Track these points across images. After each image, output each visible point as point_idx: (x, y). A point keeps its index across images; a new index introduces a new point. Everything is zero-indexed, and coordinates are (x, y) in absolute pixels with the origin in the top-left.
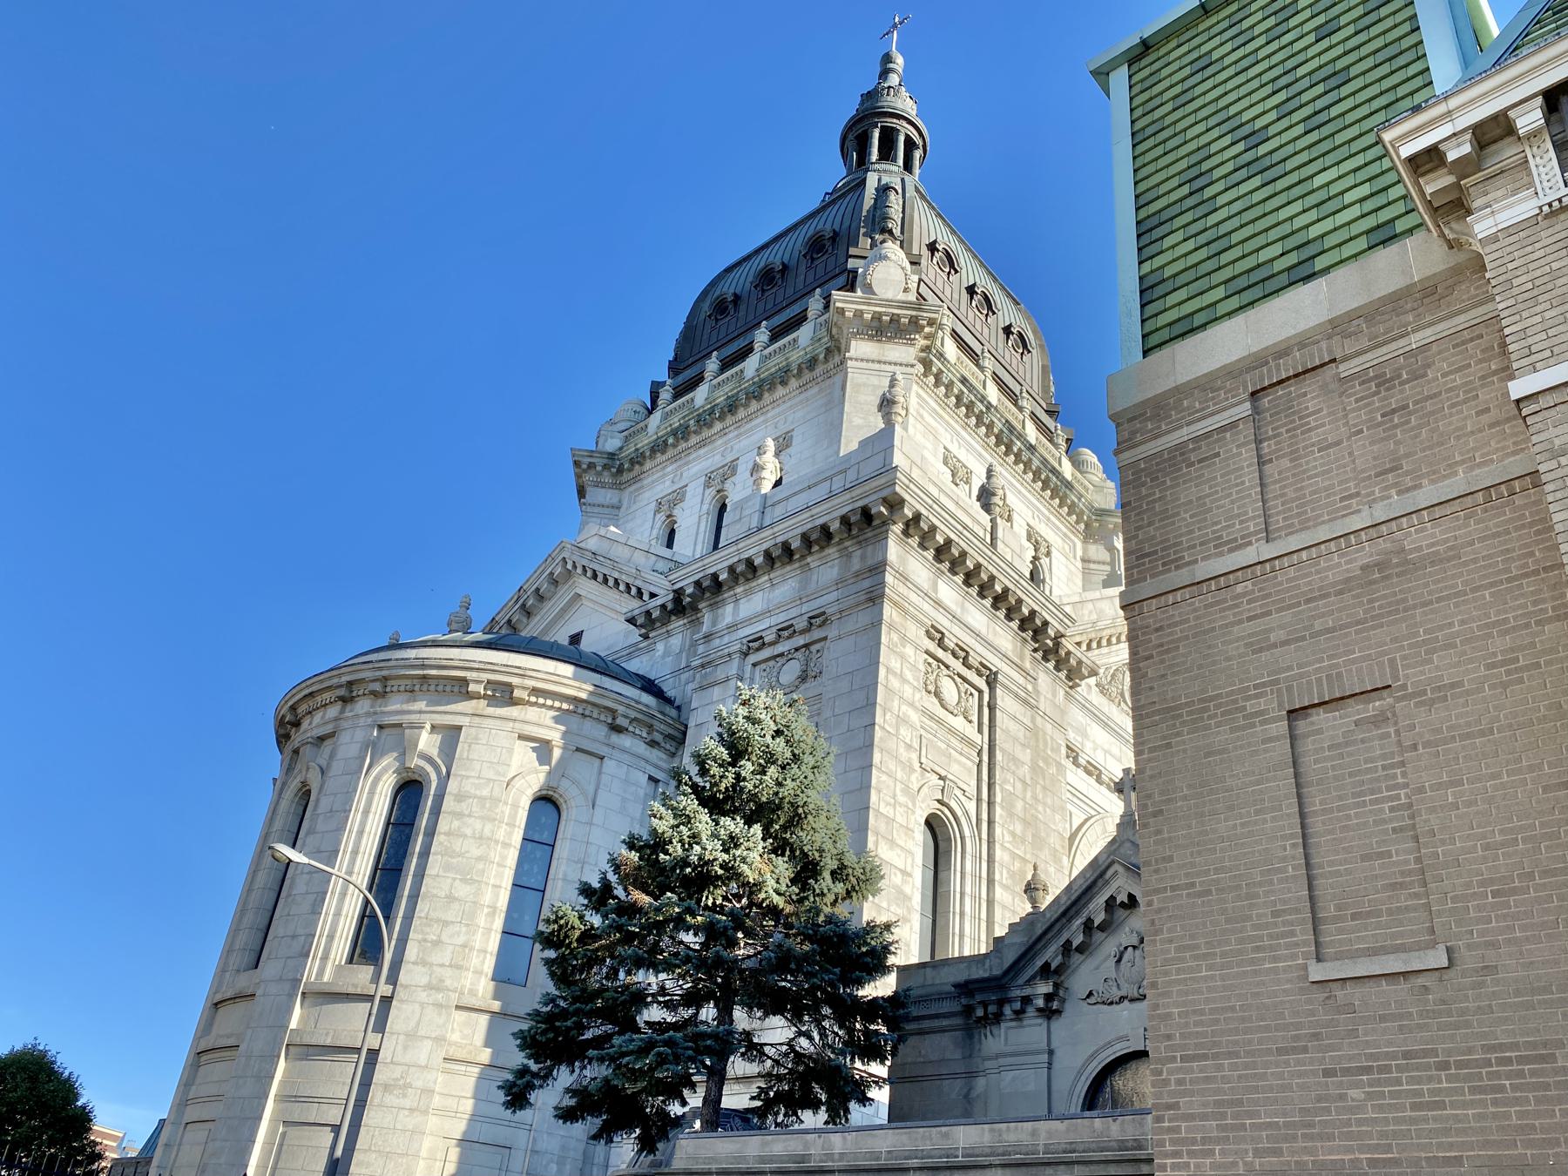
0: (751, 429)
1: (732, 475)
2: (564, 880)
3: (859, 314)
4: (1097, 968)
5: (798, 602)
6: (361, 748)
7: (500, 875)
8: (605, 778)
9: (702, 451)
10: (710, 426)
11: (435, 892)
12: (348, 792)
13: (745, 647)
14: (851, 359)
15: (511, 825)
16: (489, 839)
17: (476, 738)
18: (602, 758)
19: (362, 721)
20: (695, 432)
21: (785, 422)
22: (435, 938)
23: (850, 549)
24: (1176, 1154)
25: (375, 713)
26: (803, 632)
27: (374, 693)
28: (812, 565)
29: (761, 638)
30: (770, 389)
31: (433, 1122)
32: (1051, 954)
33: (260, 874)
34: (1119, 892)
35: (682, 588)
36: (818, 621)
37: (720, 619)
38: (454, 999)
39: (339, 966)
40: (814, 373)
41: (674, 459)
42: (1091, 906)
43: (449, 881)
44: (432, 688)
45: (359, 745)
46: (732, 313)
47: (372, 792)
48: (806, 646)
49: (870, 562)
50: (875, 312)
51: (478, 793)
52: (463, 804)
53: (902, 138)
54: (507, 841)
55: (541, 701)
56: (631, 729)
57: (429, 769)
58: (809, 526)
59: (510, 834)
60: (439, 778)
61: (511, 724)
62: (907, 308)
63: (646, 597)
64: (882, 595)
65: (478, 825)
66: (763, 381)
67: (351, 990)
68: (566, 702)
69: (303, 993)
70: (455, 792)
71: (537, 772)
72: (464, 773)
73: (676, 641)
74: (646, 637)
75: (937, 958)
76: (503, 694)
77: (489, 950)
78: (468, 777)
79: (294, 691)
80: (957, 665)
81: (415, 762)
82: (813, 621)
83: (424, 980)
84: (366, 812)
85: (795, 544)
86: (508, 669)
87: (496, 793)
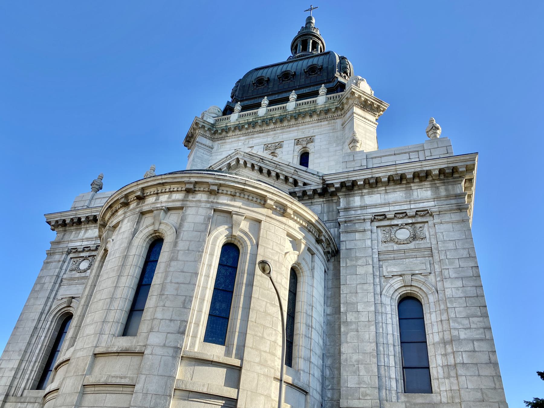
0: (290, 131)
1: (280, 148)
3: (360, 97)
6: (204, 219)
9: (261, 135)
10: (268, 124)
12: (199, 241)
14: (355, 113)
17: (269, 228)
20: (260, 126)
21: (309, 132)
25: (212, 202)
28: (413, 188)
30: (304, 117)
35: (333, 184)
37: (351, 202)
43: (264, 303)
45: (203, 217)
50: (365, 98)
51: (273, 257)
53: (319, 47)
57: (245, 237)
60: (252, 245)
61: (284, 226)
62: (376, 101)
63: (300, 184)
67: (215, 359)
68: (305, 222)
72: (265, 245)
73: (317, 208)
76: (282, 210)
78: (268, 248)
81: (236, 233)
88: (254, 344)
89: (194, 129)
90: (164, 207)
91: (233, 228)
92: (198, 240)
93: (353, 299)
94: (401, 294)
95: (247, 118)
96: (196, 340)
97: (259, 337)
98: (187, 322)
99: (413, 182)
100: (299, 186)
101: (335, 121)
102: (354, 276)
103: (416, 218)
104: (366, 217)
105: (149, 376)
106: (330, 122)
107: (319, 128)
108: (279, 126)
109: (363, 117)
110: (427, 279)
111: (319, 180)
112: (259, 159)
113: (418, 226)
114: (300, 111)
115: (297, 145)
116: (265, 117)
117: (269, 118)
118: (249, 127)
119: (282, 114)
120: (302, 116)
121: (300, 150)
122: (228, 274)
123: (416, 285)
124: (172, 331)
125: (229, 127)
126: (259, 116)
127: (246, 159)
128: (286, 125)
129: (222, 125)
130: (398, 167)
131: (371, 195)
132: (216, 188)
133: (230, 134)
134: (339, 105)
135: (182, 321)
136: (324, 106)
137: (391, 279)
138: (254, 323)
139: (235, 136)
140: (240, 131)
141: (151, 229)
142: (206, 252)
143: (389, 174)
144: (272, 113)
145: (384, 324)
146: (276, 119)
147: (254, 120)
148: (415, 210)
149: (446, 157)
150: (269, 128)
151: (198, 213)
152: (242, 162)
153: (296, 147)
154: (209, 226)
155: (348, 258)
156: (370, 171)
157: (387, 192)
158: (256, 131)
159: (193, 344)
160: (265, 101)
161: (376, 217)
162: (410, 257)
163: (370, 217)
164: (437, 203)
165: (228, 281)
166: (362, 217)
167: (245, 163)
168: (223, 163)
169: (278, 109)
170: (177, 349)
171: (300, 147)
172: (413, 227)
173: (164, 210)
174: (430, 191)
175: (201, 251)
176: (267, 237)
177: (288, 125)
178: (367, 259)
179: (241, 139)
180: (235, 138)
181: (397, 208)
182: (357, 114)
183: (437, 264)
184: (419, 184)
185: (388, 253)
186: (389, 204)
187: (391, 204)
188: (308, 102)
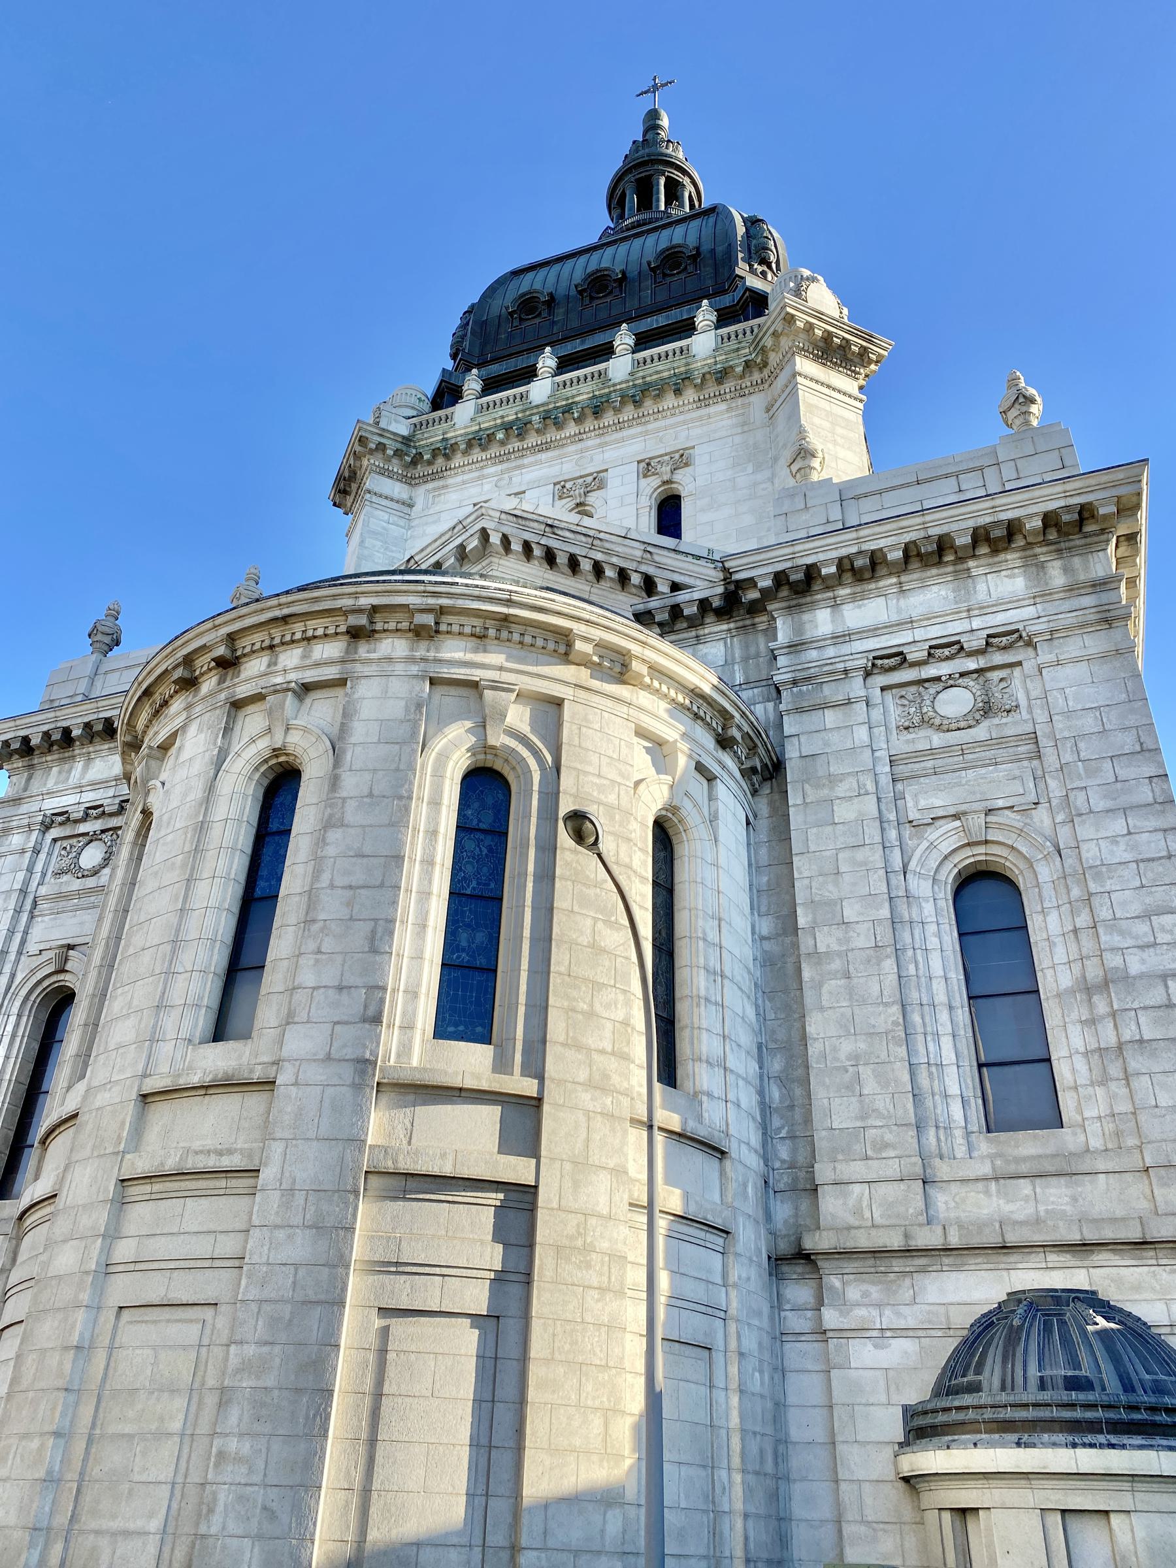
1: (599, 488)
3: (810, 327)
9: (543, 456)
10: (559, 426)
12: (397, 770)
14: (800, 375)
17: (586, 719)
20: (538, 431)
28: (974, 572)
35: (751, 579)
37: (807, 626)
41: (499, 459)
43: (589, 922)
45: (403, 703)
50: (826, 330)
51: (602, 797)
53: (686, 195)
61: (625, 709)
63: (663, 587)
66: (650, 384)
67: (470, 1083)
68: (682, 692)
72: (579, 767)
73: (714, 651)
78: (586, 773)
81: (499, 739)
83: (582, 1076)
88: (571, 1034)
89: (357, 456)
90: (293, 684)
91: (488, 727)
92: (393, 767)
93: (830, 891)
94: (960, 866)
95: (501, 413)
96: (412, 1037)
97: (582, 1012)
98: (384, 989)
99: (974, 556)
100: (658, 593)
101: (745, 400)
102: (829, 829)
103: (988, 656)
104: (849, 665)
105: (294, 1142)
106: (734, 405)
107: (702, 425)
108: (592, 428)
109: (822, 384)
110: (1028, 821)
111: (713, 573)
112: (543, 527)
113: (995, 675)
114: (648, 379)
115: (645, 476)
116: (551, 406)
117: (562, 406)
118: (507, 436)
119: (597, 393)
120: (653, 393)
121: (655, 490)
122: (485, 851)
123: (1001, 839)
124: (345, 1018)
125: (453, 441)
126: (533, 404)
127: (506, 530)
128: (611, 423)
129: (433, 437)
130: (928, 518)
131: (860, 602)
132: (429, 619)
133: (458, 460)
134: (753, 355)
135: (372, 987)
136: (713, 360)
137: (929, 829)
138: (566, 978)
139: (470, 467)
140: (483, 450)
141: (263, 744)
142: (418, 799)
143: (907, 538)
144: (569, 392)
145: (919, 952)
146: (582, 408)
147: (520, 415)
148: (984, 633)
149: (1060, 479)
150: (563, 436)
151: (386, 692)
152: (495, 539)
153: (643, 482)
154: (420, 725)
155: (807, 781)
156: (854, 535)
157: (904, 588)
158: (528, 448)
159: (405, 1049)
160: (547, 361)
161: (879, 662)
162: (980, 763)
164: (1044, 610)
165: (485, 870)
166: (841, 666)
167: (506, 541)
168: (444, 545)
169: (586, 378)
170: (365, 1065)
171: (654, 482)
172: (981, 680)
173: (294, 692)
174: (1022, 578)
175: (406, 795)
176: (583, 745)
177: (616, 421)
178: (861, 779)
179: (488, 474)
180: (470, 471)
181: (935, 632)
182: (806, 377)
183: (1053, 778)
184: (991, 560)
185: (916, 757)
186: (912, 622)
187: (915, 621)
188: (667, 352)
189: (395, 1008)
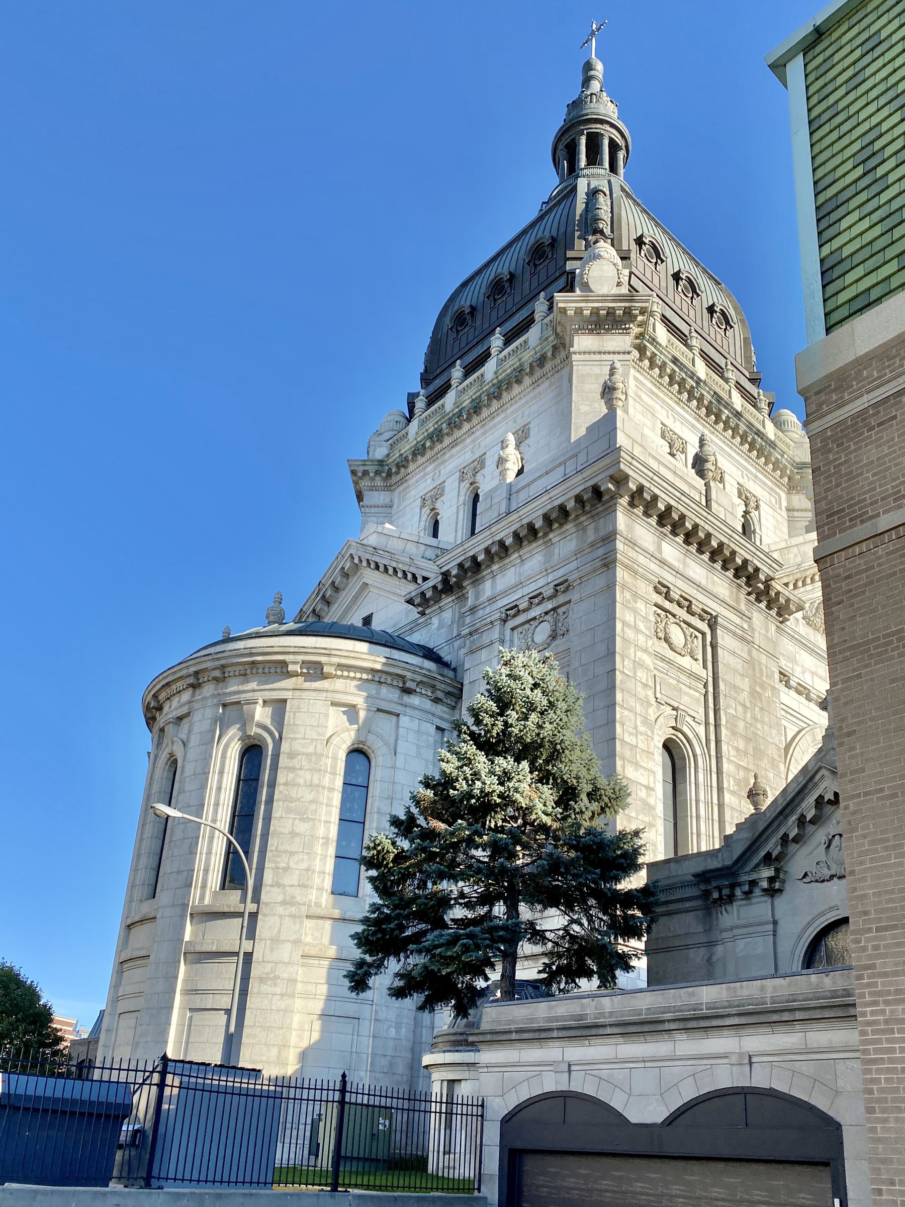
2: (379, 813)
4: (811, 853)
5: (545, 573)
7: (329, 813)
8: (402, 731)
11: (281, 830)
12: (205, 759)
13: (504, 615)
15: (334, 773)
16: (318, 786)
17: (299, 708)
18: (398, 715)
19: (209, 702)
22: (284, 865)
23: (585, 524)
24: (875, 1003)
26: (550, 598)
27: (216, 679)
28: (554, 541)
29: (516, 606)
31: (298, 1003)
32: (772, 846)
33: (147, 826)
34: (827, 792)
36: (562, 587)
38: (304, 909)
39: (215, 892)
40: (544, 369)
42: (804, 805)
43: (291, 821)
44: (260, 671)
45: (209, 721)
46: (470, 323)
47: (224, 757)
48: (554, 609)
49: (603, 533)
51: (305, 750)
52: (295, 760)
54: (331, 786)
55: (345, 674)
56: (418, 690)
58: (549, 507)
59: (333, 781)
61: (324, 694)
64: (615, 561)
65: (308, 776)
66: (500, 382)
67: (226, 910)
69: (191, 914)
70: (287, 751)
71: (348, 730)
72: (292, 736)
74: (423, 614)
75: (679, 855)
76: (315, 671)
77: (327, 871)
78: (296, 739)
79: (154, 683)
80: (682, 613)
81: (254, 730)
82: (558, 588)
83: (280, 898)
84: (221, 773)
85: (538, 524)
86: (316, 651)
87: (319, 750)
97: (283, 869)
109: (594, 353)
118: (433, 442)
163: (497, 616)
176: (296, 723)
182: (580, 353)
189: (198, 877)
